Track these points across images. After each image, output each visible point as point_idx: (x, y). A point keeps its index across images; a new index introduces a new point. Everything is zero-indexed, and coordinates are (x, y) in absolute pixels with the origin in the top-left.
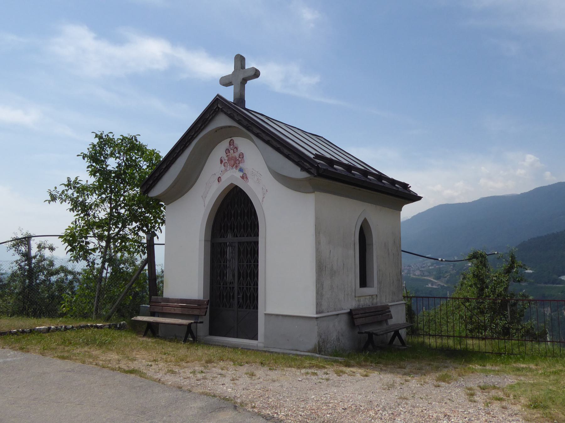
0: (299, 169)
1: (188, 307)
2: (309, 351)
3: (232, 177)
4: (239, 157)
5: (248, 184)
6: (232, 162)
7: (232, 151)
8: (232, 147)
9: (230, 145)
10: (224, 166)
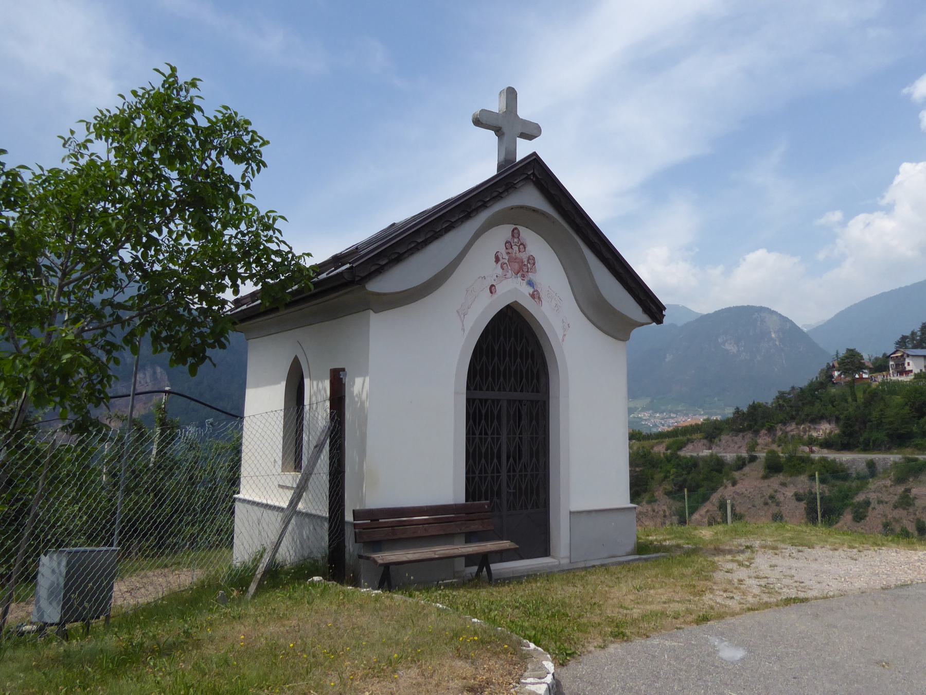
0: (640, 309)
1: (440, 521)
2: (628, 555)
3: (512, 290)
4: (528, 262)
5: (543, 308)
6: (517, 266)
7: (516, 248)
8: (516, 240)
9: (513, 236)
10: (502, 267)
